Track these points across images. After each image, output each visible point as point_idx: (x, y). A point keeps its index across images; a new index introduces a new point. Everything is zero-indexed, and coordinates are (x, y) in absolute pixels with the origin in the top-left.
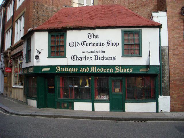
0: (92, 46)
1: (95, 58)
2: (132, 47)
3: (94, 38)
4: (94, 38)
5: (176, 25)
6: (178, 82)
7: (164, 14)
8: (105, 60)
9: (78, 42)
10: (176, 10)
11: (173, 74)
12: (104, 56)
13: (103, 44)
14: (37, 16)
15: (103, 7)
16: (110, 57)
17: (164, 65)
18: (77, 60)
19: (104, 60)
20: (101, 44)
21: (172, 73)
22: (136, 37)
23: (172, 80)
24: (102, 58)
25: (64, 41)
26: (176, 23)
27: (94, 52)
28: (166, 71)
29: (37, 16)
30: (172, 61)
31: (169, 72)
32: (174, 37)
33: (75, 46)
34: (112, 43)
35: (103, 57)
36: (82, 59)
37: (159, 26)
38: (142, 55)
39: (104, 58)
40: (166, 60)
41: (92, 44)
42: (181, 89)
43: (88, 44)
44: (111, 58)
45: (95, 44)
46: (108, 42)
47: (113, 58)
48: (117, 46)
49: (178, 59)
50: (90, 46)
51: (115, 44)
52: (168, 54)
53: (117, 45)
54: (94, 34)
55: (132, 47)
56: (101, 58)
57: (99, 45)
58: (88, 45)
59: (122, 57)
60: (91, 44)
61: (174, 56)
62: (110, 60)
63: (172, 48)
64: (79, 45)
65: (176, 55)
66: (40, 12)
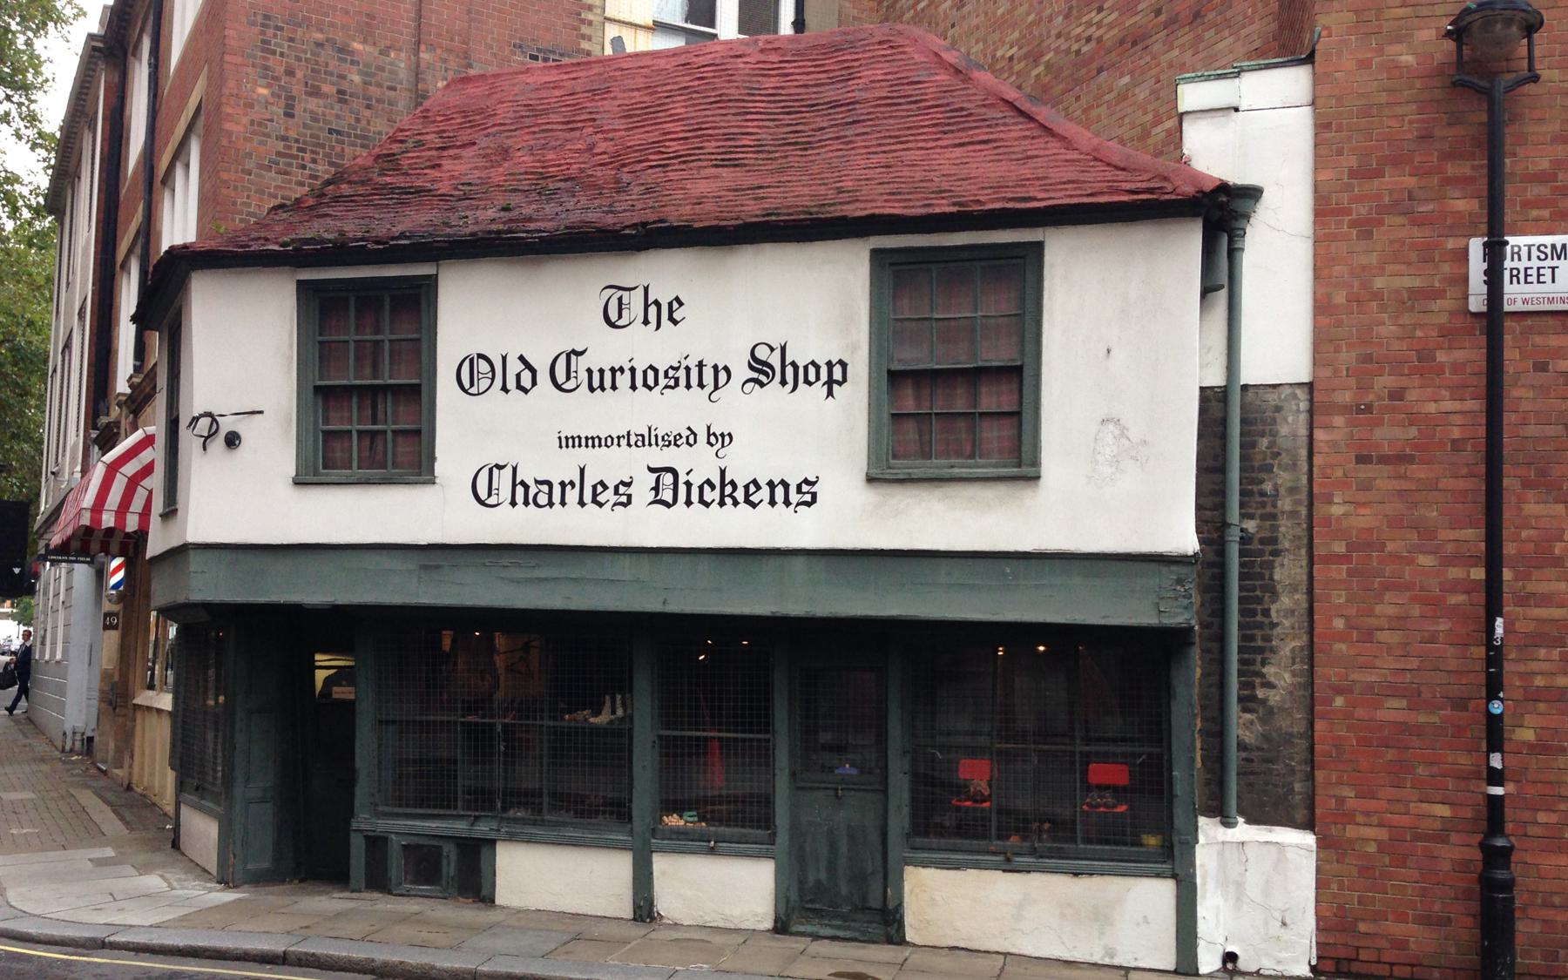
0: (633, 387)
1: (656, 489)
2: (957, 393)
3: (646, 322)
4: (646, 322)
5: (1397, 181)
6: (1394, 710)
7: (1293, 82)
8: (736, 503)
9: (522, 358)
10: (1398, 39)
11: (1342, 637)
12: (723, 472)
13: (722, 373)
14: (284, 138)
15: (774, 58)
16: (771, 484)
17: (1261, 553)
18: (513, 503)
19: (722, 503)
20: (703, 376)
21: (1339, 624)
22: (997, 304)
23: (1339, 691)
24: (713, 487)
25: (420, 348)
26: (1397, 161)
27: (645, 440)
28: (1286, 601)
29: (293, 134)
30: (1336, 511)
31: (1311, 612)
32: (1377, 295)
33: (505, 389)
34: (793, 364)
35: (717, 482)
36: (557, 498)
37: (1221, 213)
38: (1036, 462)
39: (725, 490)
40: (1285, 504)
41: (633, 370)
42: (1420, 770)
43: (601, 371)
44: (780, 491)
45: (656, 371)
46: (762, 353)
47: (799, 490)
48: (830, 393)
49: (1401, 493)
50: (614, 387)
51: (812, 370)
52: (1304, 453)
53: (833, 377)
54: (646, 289)
55: (957, 393)
56: (701, 488)
57: (688, 386)
58: (601, 381)
59: (870, 480)
60: (628, 373)
61: (1366, 471)
62: (773, 503)
63: (1345, 397)
64: (534, 383)
65: (1384, 459)
66: (313, 104)
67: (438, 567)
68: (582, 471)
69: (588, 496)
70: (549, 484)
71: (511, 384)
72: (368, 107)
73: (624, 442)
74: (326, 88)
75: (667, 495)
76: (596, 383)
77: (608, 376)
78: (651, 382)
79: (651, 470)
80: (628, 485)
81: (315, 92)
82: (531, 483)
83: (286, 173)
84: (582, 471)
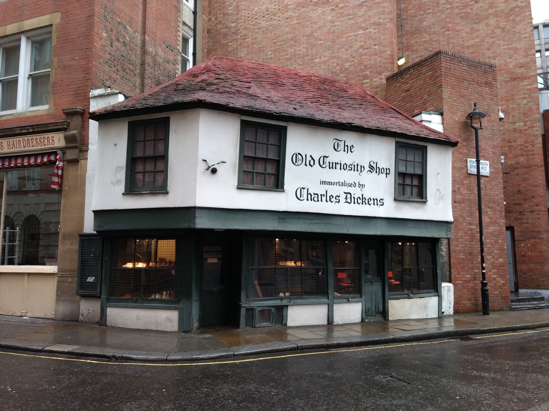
0: (341, 169)
1: (346, 198)
3: (344, 151)
4: (344, 151)
9: (311, 156)
18: (308, 200)
19: (362, 204)
27: (343, 184)
33: (306, 165)
35: (361, 198)
43: (333, 163)
50: (336, 168)
57: (354, 170)
58: (333, 166)
64: (314, 164)
67: (285, 218)
68: (327, 191)
69: (328, 199)
70: (318, 195)
71: (308, 163)
72: (131, 50)
73: (338, 184)
74: (121, 40)
75: (349, 200)
76: (331, 166)
77: (334, 164)
78: (345, 168)
79: (345, 193)
80: (339, 197)
81: (118, 40)
82: (312, 194)
83: (110, 67)
84: (327, 191)
